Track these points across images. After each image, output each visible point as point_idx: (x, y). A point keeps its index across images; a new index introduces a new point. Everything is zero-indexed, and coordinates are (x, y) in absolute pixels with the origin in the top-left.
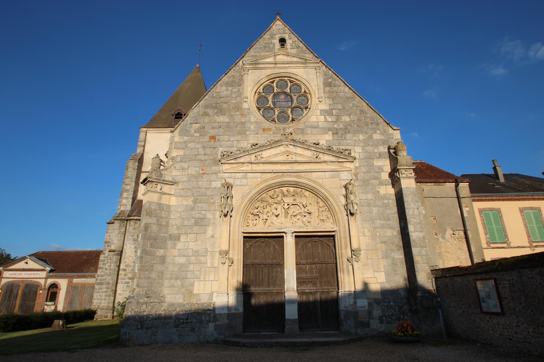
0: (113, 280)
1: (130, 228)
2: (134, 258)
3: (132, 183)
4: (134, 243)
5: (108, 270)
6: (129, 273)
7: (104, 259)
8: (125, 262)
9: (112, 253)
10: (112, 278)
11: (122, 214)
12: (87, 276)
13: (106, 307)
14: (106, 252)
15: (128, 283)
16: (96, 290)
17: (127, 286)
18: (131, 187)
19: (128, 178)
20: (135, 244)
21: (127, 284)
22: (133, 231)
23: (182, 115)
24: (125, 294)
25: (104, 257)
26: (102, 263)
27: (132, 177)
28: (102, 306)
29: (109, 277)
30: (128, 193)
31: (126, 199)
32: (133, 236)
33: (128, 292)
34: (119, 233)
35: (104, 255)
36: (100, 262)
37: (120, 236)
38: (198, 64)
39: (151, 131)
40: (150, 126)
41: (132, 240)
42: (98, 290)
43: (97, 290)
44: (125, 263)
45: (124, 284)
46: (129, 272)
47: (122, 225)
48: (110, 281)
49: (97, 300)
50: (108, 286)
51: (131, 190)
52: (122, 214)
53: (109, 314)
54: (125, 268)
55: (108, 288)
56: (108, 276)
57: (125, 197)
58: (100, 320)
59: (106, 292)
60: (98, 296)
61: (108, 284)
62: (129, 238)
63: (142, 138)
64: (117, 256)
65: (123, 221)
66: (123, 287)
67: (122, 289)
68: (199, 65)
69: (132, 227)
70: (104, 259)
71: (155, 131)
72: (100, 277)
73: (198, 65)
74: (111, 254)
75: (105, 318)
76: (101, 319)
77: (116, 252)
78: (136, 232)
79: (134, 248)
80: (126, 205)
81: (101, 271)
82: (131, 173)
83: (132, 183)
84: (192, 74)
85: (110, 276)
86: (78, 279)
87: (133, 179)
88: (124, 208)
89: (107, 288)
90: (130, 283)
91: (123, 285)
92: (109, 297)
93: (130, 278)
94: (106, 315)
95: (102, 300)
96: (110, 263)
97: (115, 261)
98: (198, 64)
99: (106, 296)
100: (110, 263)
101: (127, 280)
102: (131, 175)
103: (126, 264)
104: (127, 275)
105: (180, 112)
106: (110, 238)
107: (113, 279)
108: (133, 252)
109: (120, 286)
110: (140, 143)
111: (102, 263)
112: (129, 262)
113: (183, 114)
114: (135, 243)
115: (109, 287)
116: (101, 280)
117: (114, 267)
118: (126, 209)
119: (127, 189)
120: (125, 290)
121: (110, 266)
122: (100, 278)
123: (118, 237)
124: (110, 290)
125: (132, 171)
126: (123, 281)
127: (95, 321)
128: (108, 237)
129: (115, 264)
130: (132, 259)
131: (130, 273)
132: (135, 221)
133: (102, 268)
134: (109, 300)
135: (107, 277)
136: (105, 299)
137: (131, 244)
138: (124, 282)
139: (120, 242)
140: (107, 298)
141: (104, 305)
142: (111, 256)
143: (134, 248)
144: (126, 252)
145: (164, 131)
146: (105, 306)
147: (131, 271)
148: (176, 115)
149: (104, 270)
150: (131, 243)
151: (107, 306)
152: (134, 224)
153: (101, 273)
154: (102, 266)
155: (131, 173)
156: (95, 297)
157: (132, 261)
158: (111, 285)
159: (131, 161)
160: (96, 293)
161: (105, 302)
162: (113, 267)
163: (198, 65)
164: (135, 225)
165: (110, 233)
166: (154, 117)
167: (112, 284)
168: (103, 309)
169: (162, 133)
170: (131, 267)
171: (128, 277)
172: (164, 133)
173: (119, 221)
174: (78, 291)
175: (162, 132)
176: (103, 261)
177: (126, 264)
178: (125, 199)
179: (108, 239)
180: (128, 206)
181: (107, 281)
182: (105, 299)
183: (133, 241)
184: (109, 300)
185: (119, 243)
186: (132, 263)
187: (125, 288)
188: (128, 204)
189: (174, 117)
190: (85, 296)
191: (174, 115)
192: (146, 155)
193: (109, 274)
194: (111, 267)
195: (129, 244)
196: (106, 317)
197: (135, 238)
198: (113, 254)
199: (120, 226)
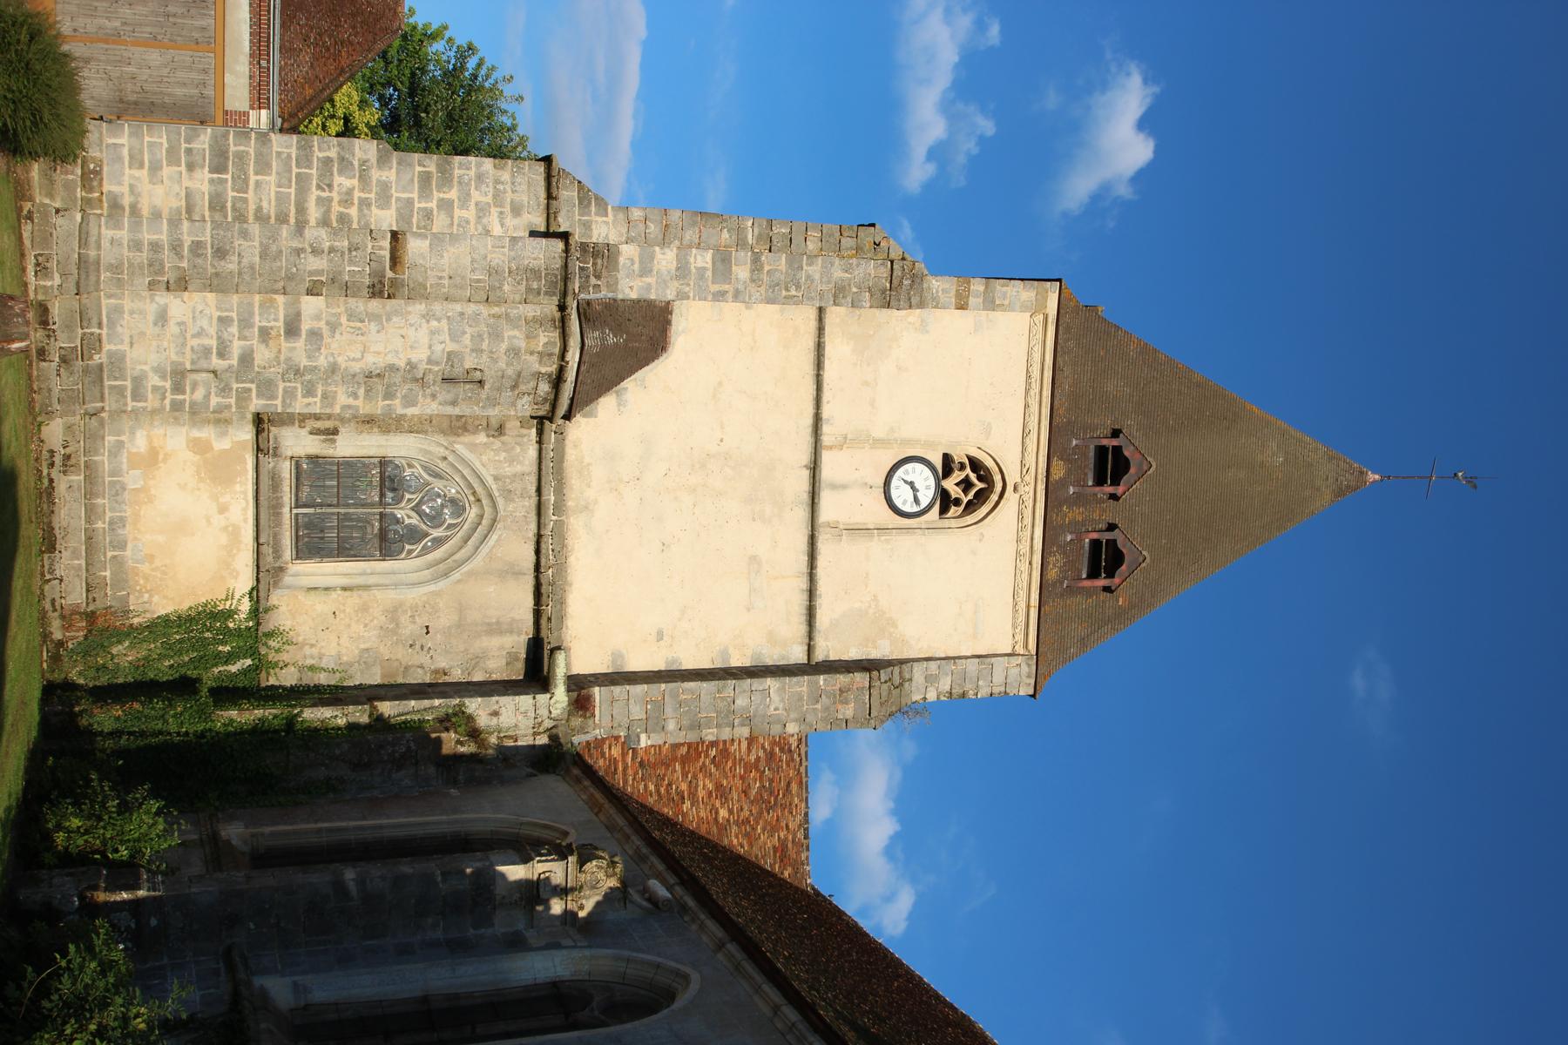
0: (240, 274)
1: (517, 327)
2: (353, 364)
3: (762, 289)
4: (436, 356)
5: (295, 244)
6: (275, 350)
7: (356, 163)
8: (334, 327)
9: (386, 254)
10: (252, 267)
11: (594, 264)
12: (264, 63)
13: (92, 253)
14: (394, 170)
15: (222, 354)
16: (188, 141)
17: (207, 351)
18: (741, 287)
19: (790, 262)
20: (430, 361)
21: (214, 351)
22: (504, 346)
23: (1116, 482)
24: (165, 344)
25: (363, 162)
26: (333, 153)
27: (798, 287)
28: (99, 233)
29: (257, 252)
30: (709, 273)
31: (678, 269)
32: (477, 351)
33: (174, 357)
34: (493, 271)
35: (374, 160)
36: (339, 145)
37: (478, 281)
38: (1377, 477)
39: (1040, 336)
40: (1068, 329)
41: (451, 347)
42: (189, 151)
43: (184, 146)
44: (328, 323)
45: (219, 338)
46: (280, 351)
47: (535, 285)
48: (235, 258)
49: (129, 150)
50: (209, 250)
51: (726, 287)
52: (599, 261)
53: (57, 276)
54: (305, 326)
55: (199, 256)
56: (261, 243)
57: (692, 260)
58: (26, 235)
59: (176, 248)
60: (151, 152)
61: (221, 253)
62: (464, 333)
63: (1005, 294)
64: (367, 281)
65: (560, 285)
66: (200, 333)
67: (192, 330)
68: (1375, 481)
69: (522, 344)
70: (356, 163)
71: (1037, 356)
72: (259, 155)
73: (1373, 477)
74: (381, 248)
75: (38, 264)
76: (27, 243)
77: (389, 274)
78: (495, 361)
79: (409, 363)
80: (645, 271)
81: (289, 156)
82: (817, 277)
83: (762, 289)
84: (1331, 459)
85: (264, 255)
86: (247, 8)
87: (787, 289)
88: (628, 263)
89: (197, 247)
90: (220, 362)
91: (212, 331)
92: (150, 265)
93: (246, 359)
94: (48, 265)
95: (130, 231)
96: (332, 250)
97: (340, 273)
98: (1377, 477)
99: (155, 247)
100: (332, 250)
101: (237, 347)
102: (808, 277)
103: (326, 331)
104: (267, 345)
105: (1132, 470)
106: (468, 184)
107: (247, 277)
108: (391, 359)
109: (207, 311)
110: (982, 288)
111: (333, 153)
112: (334, 345)
113: (1119, 490)
114: (437, 363)
115: (200, 261)
116: (241, 157)
117: (311, 273)
118: (621, 274)
119: (734, 268)
120: (184, 345)
121: (316, 251)
122: (252, 151)
123: (473, 271)
124: (185, 264)
125: (829, 282)
126: (234, 329)
127: (20, 209)
128: (472, 173)
129: (324, 279)
130: (352, 355)
131: (273, 356)
132: (557, 350)
133: (305, 159)
134: (131, 265)
135: (256, 244)
136: (136, 245)
137: (430, 347)
138: (225, 335)
139: (446, 282)
140: (145, 255)
141: (105, 244)
142: (370, 247)
143: (409, 363)
144: (389, 319)
145: (1034, 408)
146: (99, 247)
147: (289, 359)
148: (1117, 450)
149: (295, 170)
150: (438, 348)
151: (98, 263)
152: (540, 349)
153: (279, 154)
154: (318, 154)
155: (817, 277)
156: (147, 139)
157: (340, 360)
158: (210, 270)
159: (882, 269)
160: (169, 140)
161: (120, 244)
162: (309, 268)
163: (1373, 477)
164: (532, 353)
165: (497, 182)
166: (1117, 328)
167: (217, 274)
168: (83, 241)
169: (1027, 392)
170: (309, 357)
171: (253, 351)
172: (1026, 406)
173: (558, 264)
174: (183, 16)
175: (1032, 393)
176: (342, 159)
177: (326, 331)
178: (678, 260)
179: (462, 172)
180: (638, 283)
181: (236, 243)
182: (136, 245)
183: (449, 354)
184: (131, 265)
185: (440, 278)
186: (331, 359)
187: (195, 342)
188: (649, 280)
189: (1105, 442)
190: (154, 57)
191: (1115, 442)
192: (911, 319)
193: (274, 248)
194: (311, 258)
195: (432, 333)
196: (42, 269)
197: (462, 360)
198: (380, 261)
199: (535, 273)
